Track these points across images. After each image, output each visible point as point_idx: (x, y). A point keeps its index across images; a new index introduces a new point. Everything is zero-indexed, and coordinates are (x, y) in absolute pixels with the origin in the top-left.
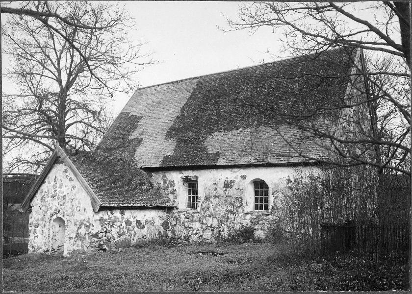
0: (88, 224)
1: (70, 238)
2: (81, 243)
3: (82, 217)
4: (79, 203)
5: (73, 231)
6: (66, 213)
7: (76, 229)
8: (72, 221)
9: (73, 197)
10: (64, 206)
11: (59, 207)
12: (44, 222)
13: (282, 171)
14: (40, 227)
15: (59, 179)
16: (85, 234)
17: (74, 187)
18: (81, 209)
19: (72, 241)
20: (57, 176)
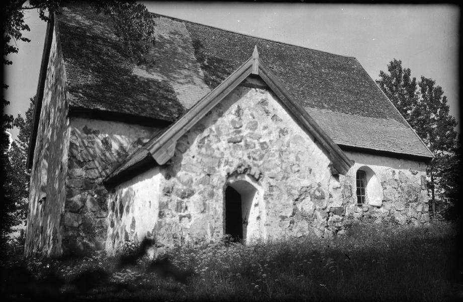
0: (318, 194)
1: (283, 218)
2: (307, 224)
3: (306, 183)
4: (297, 159)
5: (285, 206)
6: (267, 173)
7: (291, 202)
8: (282, 187)
9: (284, 149)
10: (261, 162)
11: (250, 162)
12: (210, 188)
13: (387, 162)
14: (196, 197)
15: (246, 111)
16: (315, 209)
17: (283, 132)
18: (302, 167)
19: (287, 223)
20: (243, 106)
